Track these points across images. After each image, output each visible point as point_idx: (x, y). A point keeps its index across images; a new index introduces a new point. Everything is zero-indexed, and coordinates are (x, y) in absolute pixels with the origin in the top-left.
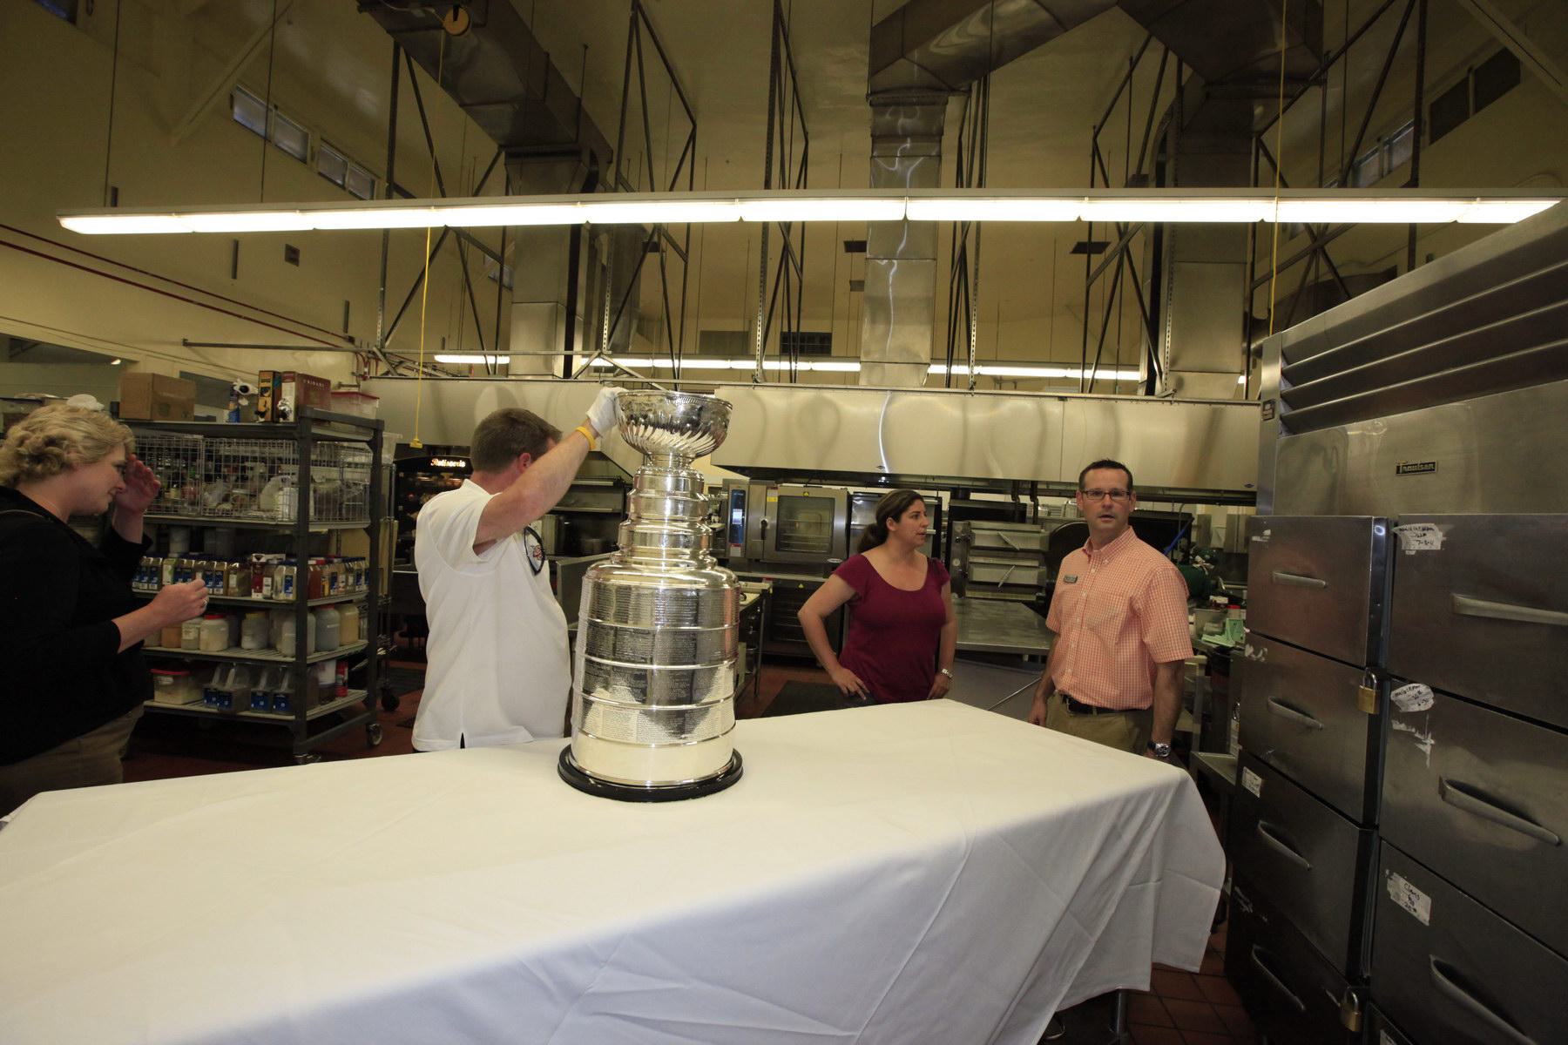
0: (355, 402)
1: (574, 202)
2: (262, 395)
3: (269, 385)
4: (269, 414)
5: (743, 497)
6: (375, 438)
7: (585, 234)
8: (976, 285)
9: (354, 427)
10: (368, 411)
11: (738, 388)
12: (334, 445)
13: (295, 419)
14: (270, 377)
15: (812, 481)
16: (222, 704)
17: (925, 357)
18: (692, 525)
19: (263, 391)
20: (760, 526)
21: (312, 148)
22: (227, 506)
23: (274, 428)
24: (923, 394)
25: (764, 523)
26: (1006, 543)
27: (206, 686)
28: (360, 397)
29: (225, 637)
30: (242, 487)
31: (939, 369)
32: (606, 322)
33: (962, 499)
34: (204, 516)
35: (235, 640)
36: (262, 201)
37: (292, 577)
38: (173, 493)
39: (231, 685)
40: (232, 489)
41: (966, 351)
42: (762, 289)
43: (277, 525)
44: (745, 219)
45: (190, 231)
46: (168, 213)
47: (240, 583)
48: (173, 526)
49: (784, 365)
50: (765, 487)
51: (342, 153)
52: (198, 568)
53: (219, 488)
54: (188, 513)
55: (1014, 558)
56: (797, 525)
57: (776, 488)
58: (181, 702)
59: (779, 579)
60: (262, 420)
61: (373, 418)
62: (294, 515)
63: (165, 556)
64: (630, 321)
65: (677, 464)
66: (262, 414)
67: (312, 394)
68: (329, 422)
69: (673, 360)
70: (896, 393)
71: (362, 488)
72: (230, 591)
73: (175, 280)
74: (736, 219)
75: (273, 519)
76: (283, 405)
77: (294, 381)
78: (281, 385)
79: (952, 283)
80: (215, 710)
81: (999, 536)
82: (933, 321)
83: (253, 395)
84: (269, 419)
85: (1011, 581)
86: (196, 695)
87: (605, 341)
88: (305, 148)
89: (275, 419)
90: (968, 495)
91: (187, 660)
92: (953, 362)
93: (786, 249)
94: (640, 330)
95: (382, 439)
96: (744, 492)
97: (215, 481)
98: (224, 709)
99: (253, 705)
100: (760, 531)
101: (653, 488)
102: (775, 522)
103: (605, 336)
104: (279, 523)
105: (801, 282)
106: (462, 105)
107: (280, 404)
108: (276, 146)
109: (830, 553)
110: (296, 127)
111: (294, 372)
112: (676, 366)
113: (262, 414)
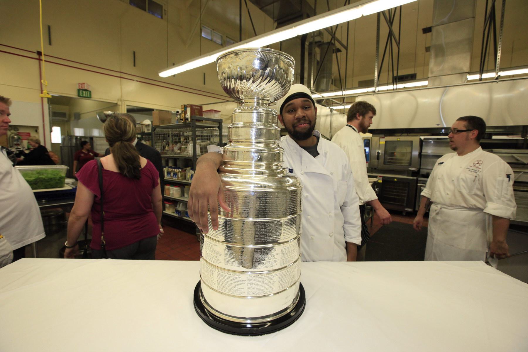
0: (212, 113)
1: (291, 28)
2: (182, 113)
3: (183, 109)
4: (184, 119)
5: (370, 142)
6: (220, 125)
7: (306, 47)
8: (502, 21)
9: (212, 122)
10: (217, 116)
11: (366, 96)
12: (211, 129)
13: (190, 120)
14: (183, 107)
15: (404, 134)
16: (179, 214)
17: (466, 69)
18: (267, 145)
19: (182, 111)
20: (377, 154)
21: (224, 40)
22: (179, 151)
23: (186, 124)
24: (464, 86)
25: (378, 153)
26: (517, 160)
27: (176, 208)
28: (213, 111)
29: (180, 193)
30: (184, 145)
31: (477, 77)
32: (312, 77)
33: (487, 139)
34: (173, 155)
35: (183, 195)
36: (201, 55)
37: (192, 174)
38: (167, 148)
39: (180, 208)
40: (182, 146)
41: (493, 62)
42: (377, 51)
43: (188, 157)
44: (365, 14)
45: (185, 70)
46: (179, 65)
47: (181, 176)
48: (169, 158)
49: (391, 87)
50: (378, 138)
51: (233, 40)
52: (172, 171)
53: (179, 145)
54: (169, 154)
55: (523, 168)
56: (395, 154)
57: (384, 138)
58: (171, 212)
59: (385, 177)
60: (182, 122)
61: (219, 119)
62: (192, 154)
63: (165, 168)
64: (329, 80)
65: (258, 103)
66: (182, 120)
67: (196, 111)
68: (202, 121)
69: (342, 91)
70: (446, 88)
71: (217, 143)
72: (179, 179)
73: (190, 87)
74: (360, 16)
75: (188, 154)
76: (187, 116)
77: (189, 107)
78: (186, 109)
79: (484, 31)
80: (177, 216)
81: (513, 157)
82: (471, 51)
83: (180, 114)
84: (184, 121)
85: (520, 180)
86: (175, 211)
87: (312, 85)
88: (222, 41)
89: (186, 121)
90: (491, 137)
91: (171, 200)
92: (484, 72)
93: (391, 34)
94: (332, 83)
95: (222, 126)
96: (369, 140)
97: (178, 143)
98: (179, 216)
99: (186, 216)
100: (377, 156)
101: (239, 122)
102: (383, 152)
103: (312, 83)
104: (189, 156)
105: (399, 48)
106: (261, 9)
107: (186, 115)
108: (215, 42)
109: (410, 164)
110: (218, 34)
111: (189, 104)
112: (344, 94)
113: (182, 120)
